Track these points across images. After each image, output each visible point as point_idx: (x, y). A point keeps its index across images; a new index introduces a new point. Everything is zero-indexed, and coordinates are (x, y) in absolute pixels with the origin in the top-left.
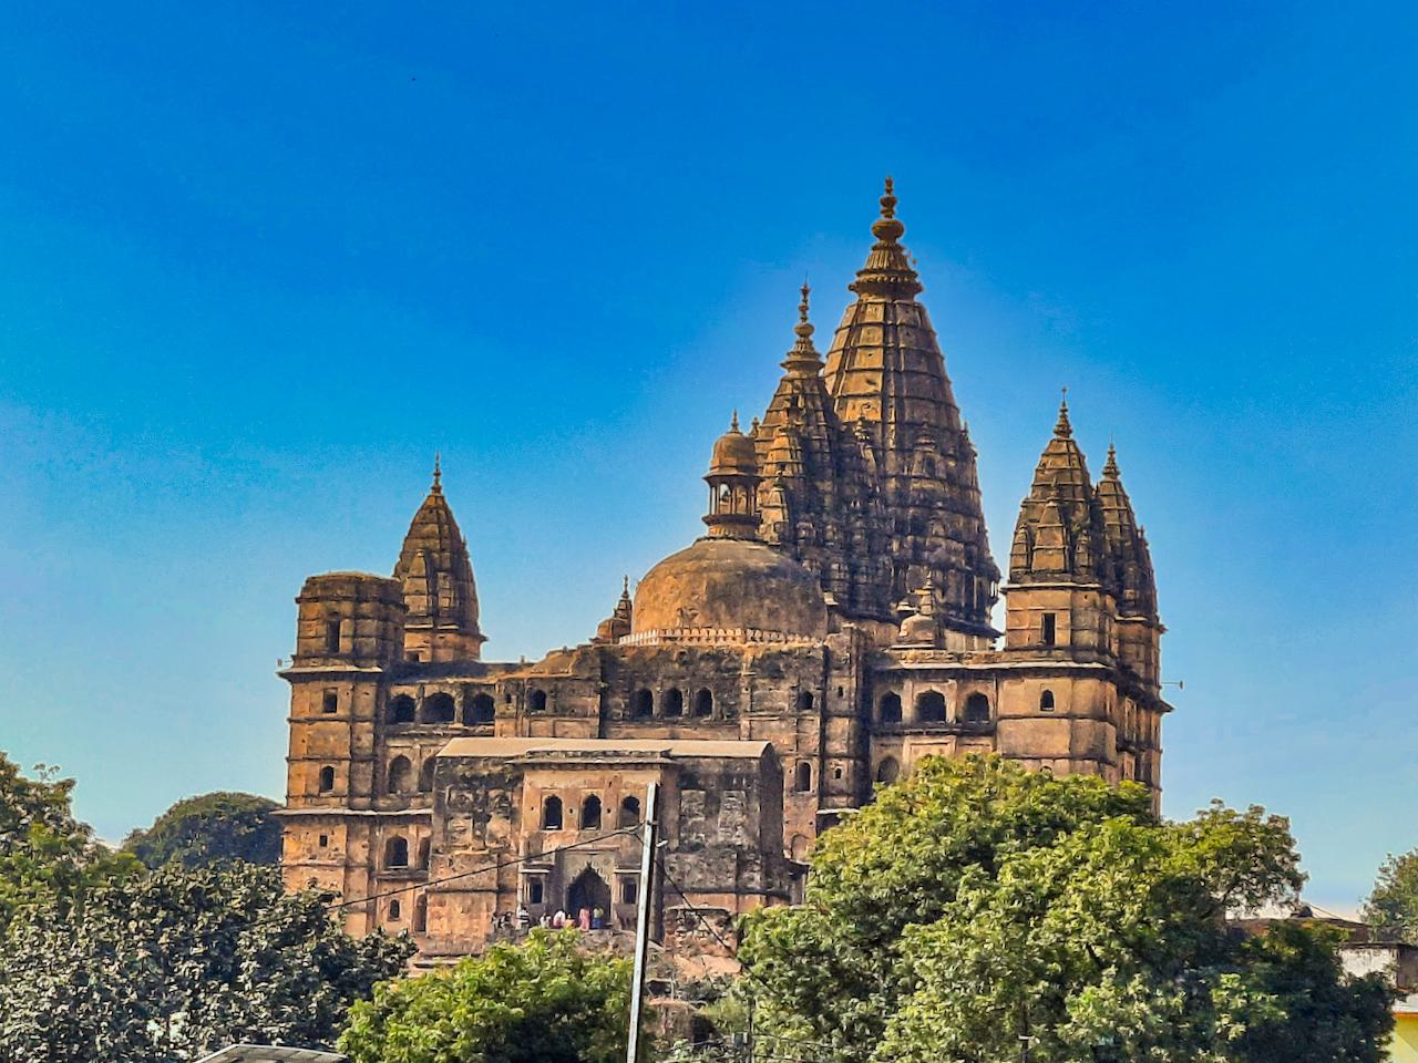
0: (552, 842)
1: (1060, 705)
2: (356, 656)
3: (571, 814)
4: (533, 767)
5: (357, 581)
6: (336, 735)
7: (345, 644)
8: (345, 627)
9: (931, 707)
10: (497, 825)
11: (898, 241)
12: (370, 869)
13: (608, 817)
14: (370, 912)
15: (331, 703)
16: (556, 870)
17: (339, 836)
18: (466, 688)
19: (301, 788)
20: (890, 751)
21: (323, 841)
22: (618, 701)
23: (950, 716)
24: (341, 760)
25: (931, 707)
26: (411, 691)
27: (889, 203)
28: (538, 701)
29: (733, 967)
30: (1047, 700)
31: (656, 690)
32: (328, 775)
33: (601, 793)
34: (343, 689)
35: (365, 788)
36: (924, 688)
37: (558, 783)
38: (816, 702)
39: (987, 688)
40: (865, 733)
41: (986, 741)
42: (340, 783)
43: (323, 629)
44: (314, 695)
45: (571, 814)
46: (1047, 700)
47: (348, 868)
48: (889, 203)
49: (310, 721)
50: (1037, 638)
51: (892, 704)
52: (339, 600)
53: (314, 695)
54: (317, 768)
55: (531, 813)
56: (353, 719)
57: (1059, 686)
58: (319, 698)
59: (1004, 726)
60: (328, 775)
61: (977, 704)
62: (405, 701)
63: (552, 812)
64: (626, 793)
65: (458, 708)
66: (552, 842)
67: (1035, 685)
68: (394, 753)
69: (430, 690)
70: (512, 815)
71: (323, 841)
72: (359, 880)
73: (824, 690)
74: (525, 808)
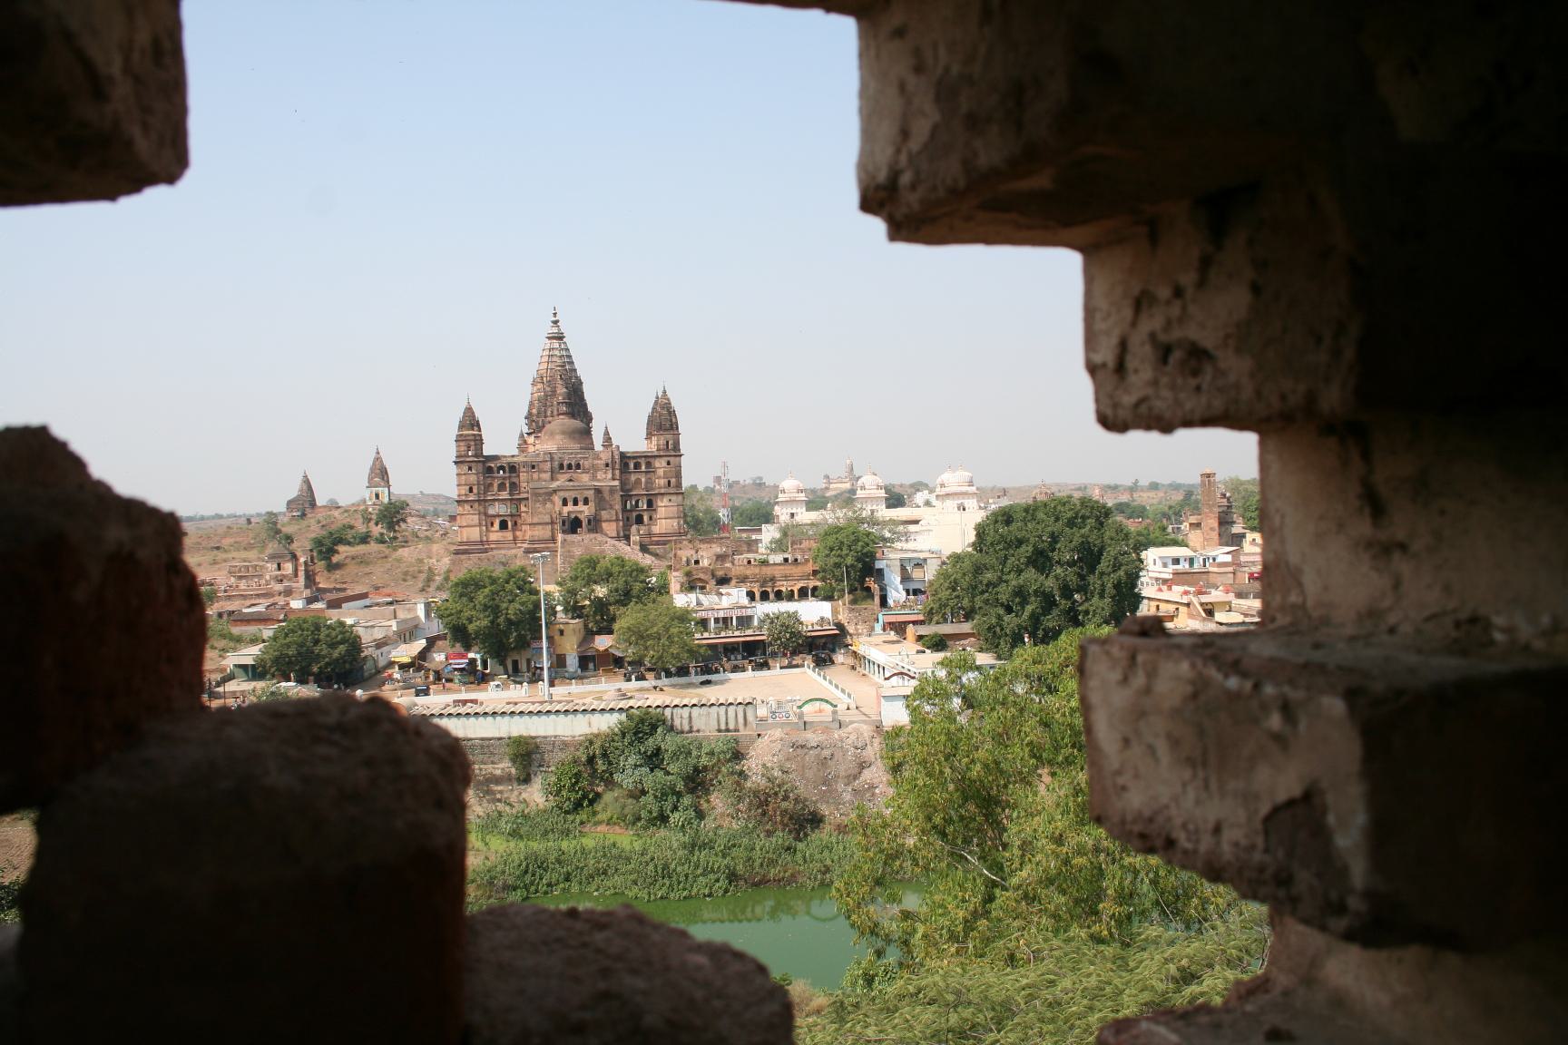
0: (566, 510)
14: (486, 526)
15: (470, 469)
17: (476, 505)
18: (509, 463)
19: (463, 492)
24: (474, 485)
26: (493, 465)
28: (533, 467)
29: (693, 552)
30: (669, 463)
31: (565, 463)
34: (473, 464)
37: (566, 494)
40: (621, 473)
42: (475, 490)
47: (479, 514)
52: (470, 440)
61: (649, 465)
63: (565, 503)
66: (566, 510)
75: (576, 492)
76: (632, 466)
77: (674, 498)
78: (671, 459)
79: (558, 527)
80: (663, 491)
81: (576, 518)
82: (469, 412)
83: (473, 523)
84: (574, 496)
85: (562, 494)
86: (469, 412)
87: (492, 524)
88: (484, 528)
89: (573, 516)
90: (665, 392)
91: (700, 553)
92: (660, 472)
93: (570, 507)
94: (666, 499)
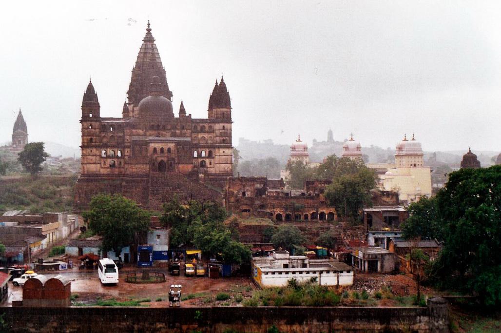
4: (151, 143)
21: (91, 151)
25: (203, 128)
27: (149, 24)
39: (212, 125)
41: (213, 134)
42: (94, 141)
48: (149, 24)
67: (222, 125)
71: (91, 151)
75: (163, 144)
76: (199, 128)
78: (226, 125)
82: (90, 89)
85: (152, 145)
86: (90, 89)
87: (105, 164)
90: (222, 80)
94: (221, 150)
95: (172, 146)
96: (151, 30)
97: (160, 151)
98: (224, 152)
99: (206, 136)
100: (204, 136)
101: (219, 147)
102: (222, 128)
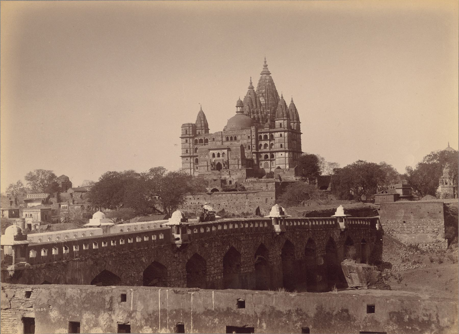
1: (283, 135)
2: (190, 135)
3: (216, 156)
5: (189, 124)
6: (188, 144)
7: (188, 133)
8: (188, 131)
9: (266, 137)
10: (207, 157)
11: (267, 67)
12: (194, 163)
13: (221, 156)
15: (187, 141)
16: (214, 163)
20: (261, 143)
21: (187, 159)
22: (224, 139)
23: (268, 138)
25: (266, 137)
27: (265, 62)
30: (281, 135)
32: (187, 151)
33: (220, 152)
34: (188, 139)
35: (192, 152)
36: (265, 134)
38: (250, 137)
39: (273, 134)
43: (185, 131)
44: (184, 140)
45: (216, 156)
46: (281, 135)
48: (265, 62)
49: (184, 144)
50: (279, 127)
51: (261, 136)
52: (187, 127)
53: (184, 140)
54: (185, 150)
55: (211, 156)
56: (190, 144)
57: (283, 133)
58: (185, 140)
59: (275, 139)
60: (187, 151)
62: (196, 140)
64: (223, 152)
65: (203, 140)
66: (214, 159)
67: (279, 133)
68: (195, 147)
69: (200, 138)
70: (209, 156)
71: (187, 159)
72: (192, 165)
73: (251, 135)
74: (210, 155)
75: (219, 151)
77: (283, 153)
79: (209, 167)
80: (277, 150)
81: (219, 163)
83: (187, 167)
84: (218, 153)
85: (211, 152)
88: (192, 170)
89: (217, 163)
91: (232, 177)
92: (277, 140)
93: (216, 158)
94: (280, 153)
95: (225, 151)
96: (267, 66)
97: (217, 155)
98: (282, 155)
99: (268, 142)
100: (267, 143)
101: (278, 152)
102: (279, 136)
